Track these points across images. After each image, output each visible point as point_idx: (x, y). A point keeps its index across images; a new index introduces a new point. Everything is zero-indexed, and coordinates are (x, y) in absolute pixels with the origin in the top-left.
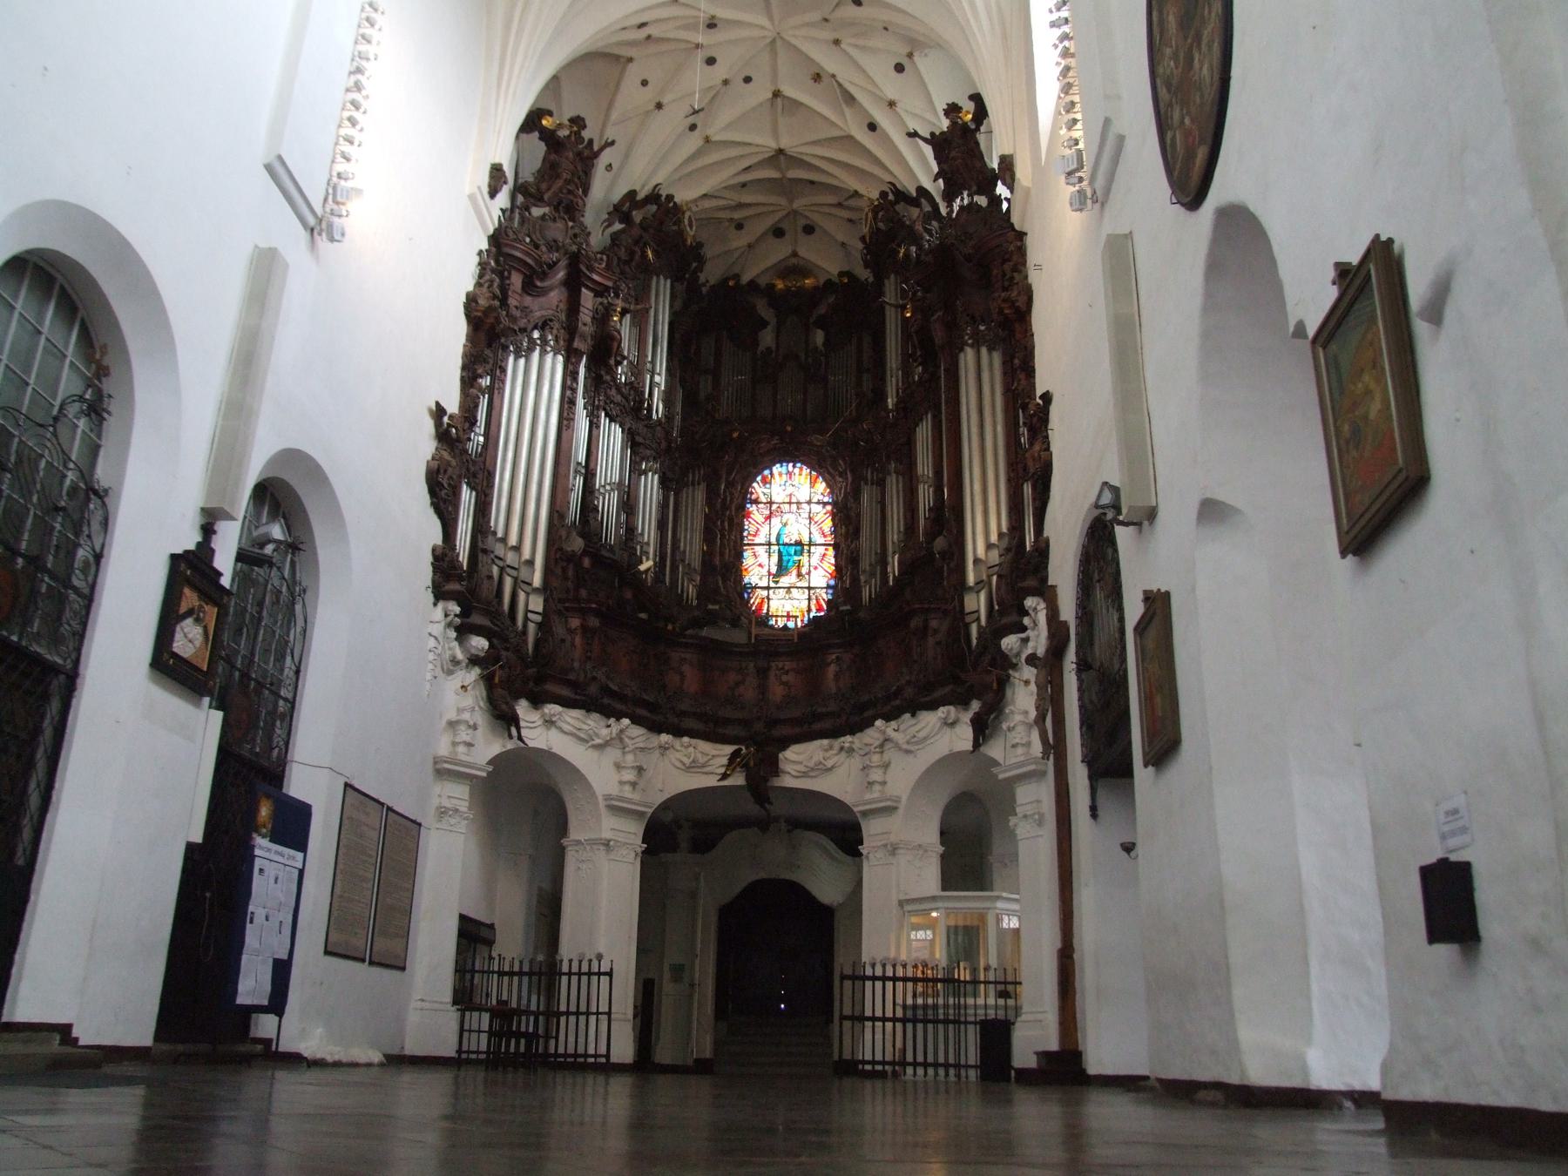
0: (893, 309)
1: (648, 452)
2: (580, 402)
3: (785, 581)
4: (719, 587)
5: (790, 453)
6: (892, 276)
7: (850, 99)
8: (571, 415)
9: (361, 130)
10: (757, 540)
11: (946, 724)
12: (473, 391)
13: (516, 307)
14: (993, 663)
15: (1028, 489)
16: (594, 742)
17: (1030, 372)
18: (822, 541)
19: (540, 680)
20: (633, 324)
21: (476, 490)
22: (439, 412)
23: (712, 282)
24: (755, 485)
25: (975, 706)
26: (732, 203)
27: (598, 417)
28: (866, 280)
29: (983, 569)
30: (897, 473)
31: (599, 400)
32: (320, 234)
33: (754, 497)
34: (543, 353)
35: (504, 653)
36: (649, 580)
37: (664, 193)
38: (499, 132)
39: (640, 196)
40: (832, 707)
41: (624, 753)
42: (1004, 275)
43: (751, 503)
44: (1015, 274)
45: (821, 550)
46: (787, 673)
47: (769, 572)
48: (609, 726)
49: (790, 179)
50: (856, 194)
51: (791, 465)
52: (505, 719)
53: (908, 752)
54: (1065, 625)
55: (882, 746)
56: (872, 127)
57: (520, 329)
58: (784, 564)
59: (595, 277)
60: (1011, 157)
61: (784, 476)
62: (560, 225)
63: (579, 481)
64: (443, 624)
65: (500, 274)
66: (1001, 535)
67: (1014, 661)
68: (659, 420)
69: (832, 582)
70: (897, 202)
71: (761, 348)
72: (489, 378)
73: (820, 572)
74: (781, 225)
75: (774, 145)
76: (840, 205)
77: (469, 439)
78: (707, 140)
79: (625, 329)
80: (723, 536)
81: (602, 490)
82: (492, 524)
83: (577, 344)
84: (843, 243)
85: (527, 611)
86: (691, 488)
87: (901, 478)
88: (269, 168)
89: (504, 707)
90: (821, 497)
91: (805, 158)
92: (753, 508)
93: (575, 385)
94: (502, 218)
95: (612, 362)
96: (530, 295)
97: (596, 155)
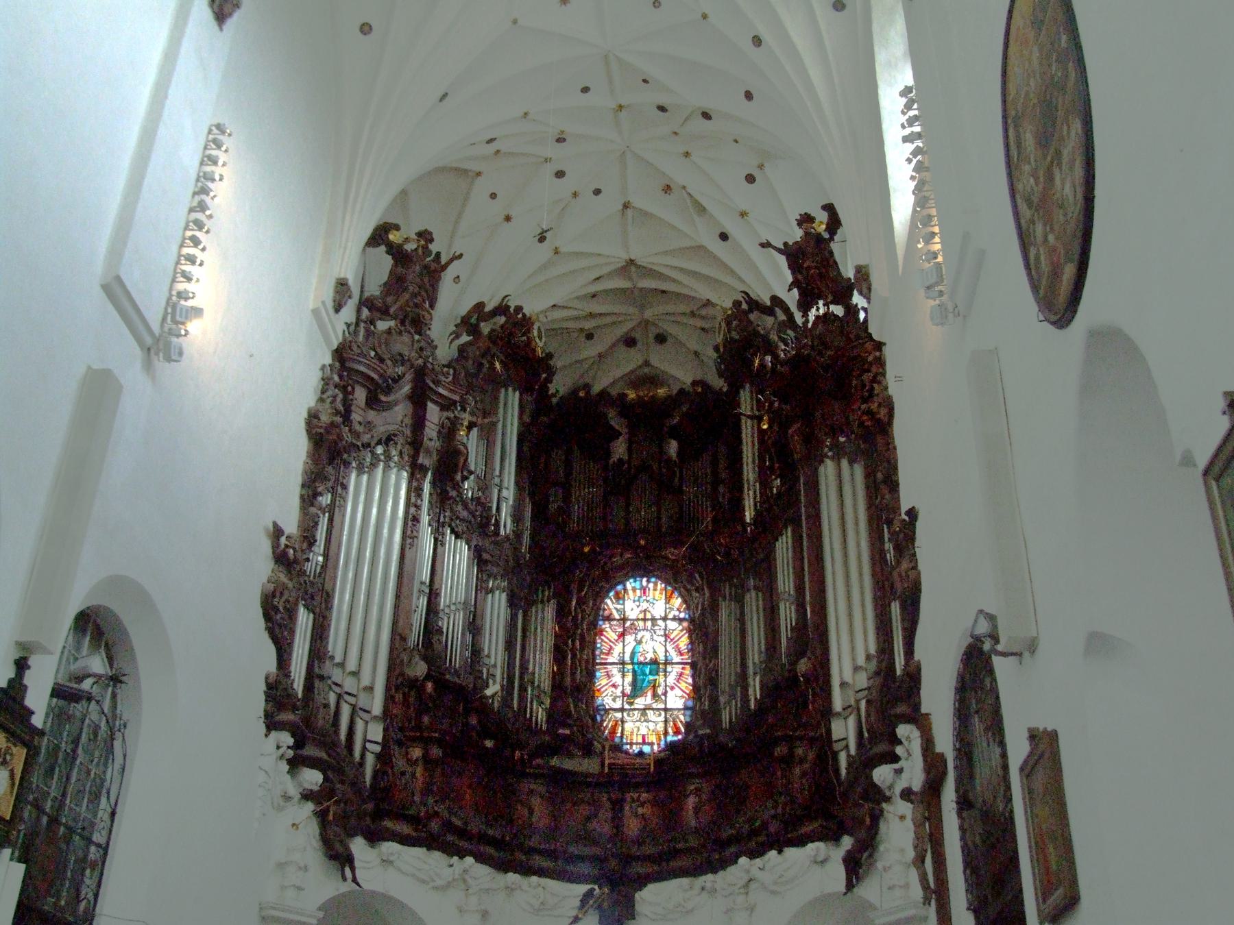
0: (749, 422)
1: (495, 570)
2: (425, 519)
3: (640, 702)
4: (571, 711)
5: (644, 567)
6: (748, 386)
7: (701, 209)
8: (415, 533)
9: (203, 249)
10: (611, 660)
11: (816, 862)
12: (313, 510)
13: (360, 423)
14: (866, 796)
15: (895, 608)
16: (435, 884)
17: (894, 486)
18: (677, 659)
19: (378, 815)
20: (480, 437)
21: (314, 613)
22: (277, 532)
23: (561, 393)
24: (608, 601)
25: (847, 842)
26: (584, 313)
27: (443, 534)
28: (721, 389)
29: (851, 693)
30: (756, 588)
31: (445, 517)
32: (157, 354)
33: (606, 613)
34: (387, 468)
35: (338, 786)
36: (496, 705)
37: (512, 305)
38: (345, 248)
39: (488, 309)
40: (693, 842)
41: (467, 895)
42: (864, 386)
44: (875, 385)
45: (678, 668)
46: (642, 805)
47: (623, 692)
48: (451, 866)
49: (641, 289)
50: (708, 303)
51: (645, 579)
52: (342, 859)
53: (773, 893)
54: (941, 758)
55: (746, 886)
56: (724, 237)
57: (363, 445)
59: (441, 390)
60: (866, 267)
61: (638, 592)
62: (406, 338)
63: (423, 602)
64: (274, 757)
65: (344, 389)
66: (868, 658)
67: (888, 794)
68: (507, 538)
69: (690, 704)
70: (751, 310)
71: (614, 458)
72: (329, 495)
73: (677, 692)
74: (633, 334)
75: (625, 256)
76: (693, 314)
77: (308, 560)
78: (556, 252)
79: (471, 442)
80: (574, 656)
81: (447, 610)
82: (330, 648)
83: (421, 460)
84: (696, 353)
85: (365, 741)
86: (540, 606)
87: (760, 594)
88: (106, 288)
89: (337, 845)
91: (655, 268)
92: (606, 626)
93: (419, 501)
94: (347, 333)
95: (458, 477)
96: (372, 409)
97: (444, 268)
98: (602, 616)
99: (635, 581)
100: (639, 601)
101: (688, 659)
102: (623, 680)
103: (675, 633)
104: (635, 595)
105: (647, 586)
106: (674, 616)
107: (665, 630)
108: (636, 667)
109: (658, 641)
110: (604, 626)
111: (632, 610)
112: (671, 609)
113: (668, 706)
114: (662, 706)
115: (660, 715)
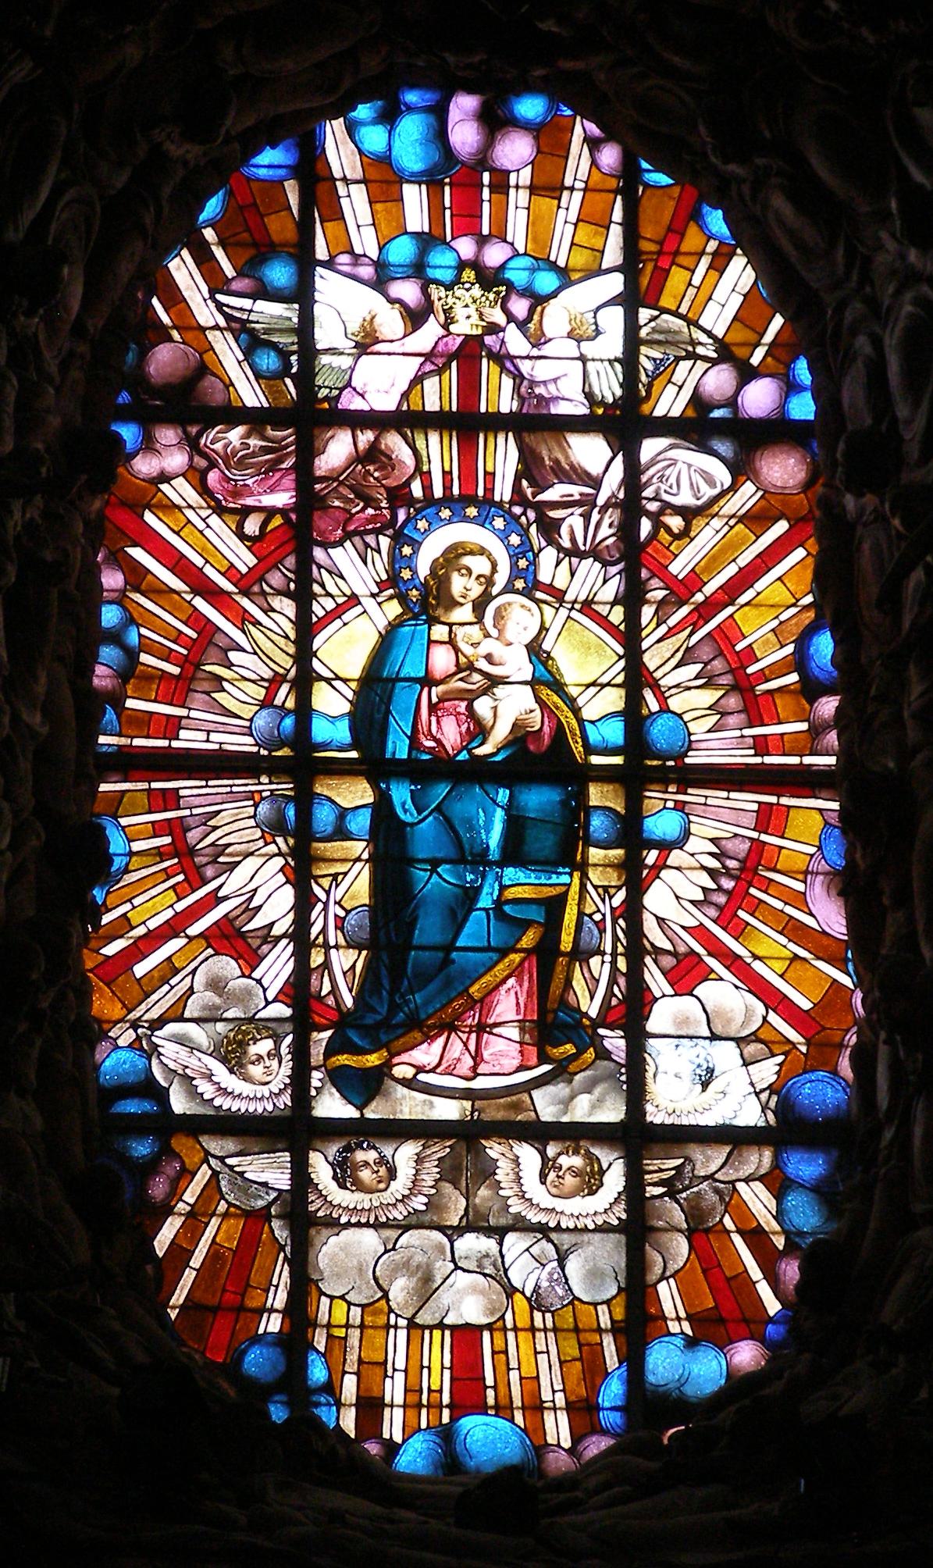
33: (164, 360)
43: (148, 420)
51: (464, 105)
58: (428, 929)
61: (414, 200)
90: (719, 380)
98: (139, 381)
99: (389, 117)
100: (418, 270)
101: (812, 740)
102: (304, 904)
103: (708, 536)
104: (390, 227)
105: (483, 159)
106: (698, 400)
107: (630, 505)
108: (401, 793)
109: (577, 591)
110: (145, 466)
111: (366, 343)
112: (667, 339)
113: (655, 1115)
114: (613, 1112)
115: (591, 1182)
